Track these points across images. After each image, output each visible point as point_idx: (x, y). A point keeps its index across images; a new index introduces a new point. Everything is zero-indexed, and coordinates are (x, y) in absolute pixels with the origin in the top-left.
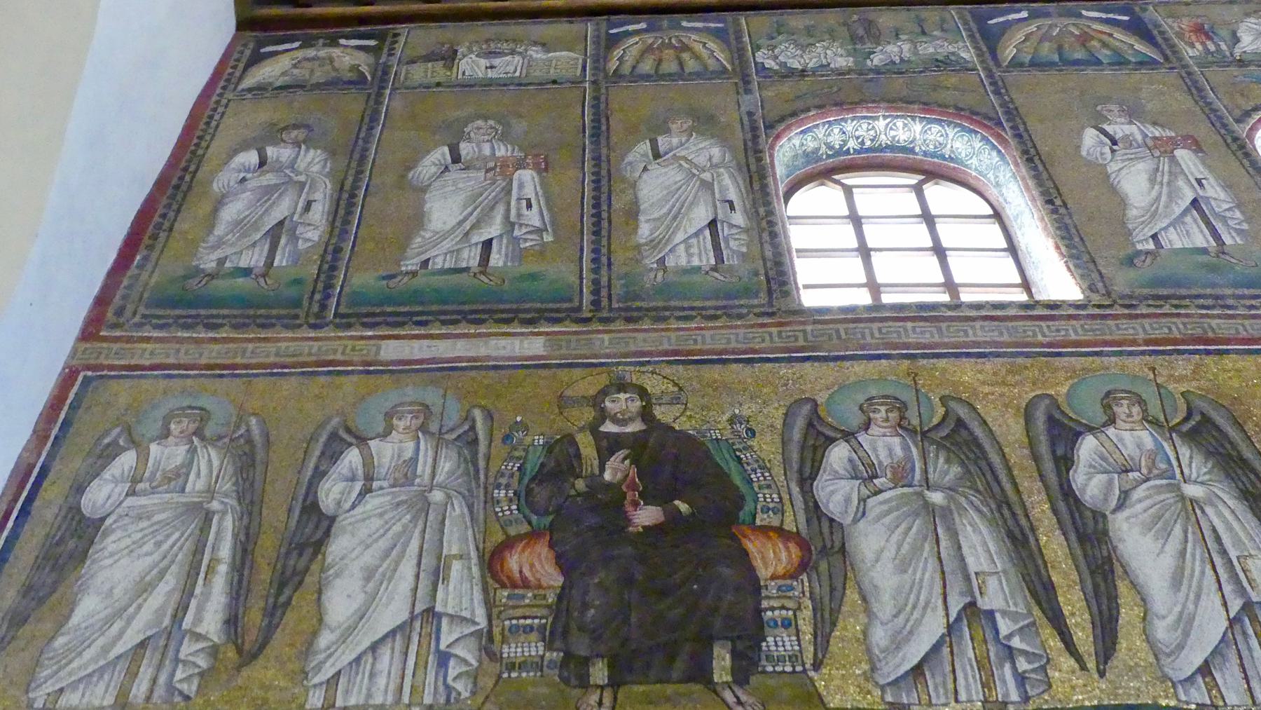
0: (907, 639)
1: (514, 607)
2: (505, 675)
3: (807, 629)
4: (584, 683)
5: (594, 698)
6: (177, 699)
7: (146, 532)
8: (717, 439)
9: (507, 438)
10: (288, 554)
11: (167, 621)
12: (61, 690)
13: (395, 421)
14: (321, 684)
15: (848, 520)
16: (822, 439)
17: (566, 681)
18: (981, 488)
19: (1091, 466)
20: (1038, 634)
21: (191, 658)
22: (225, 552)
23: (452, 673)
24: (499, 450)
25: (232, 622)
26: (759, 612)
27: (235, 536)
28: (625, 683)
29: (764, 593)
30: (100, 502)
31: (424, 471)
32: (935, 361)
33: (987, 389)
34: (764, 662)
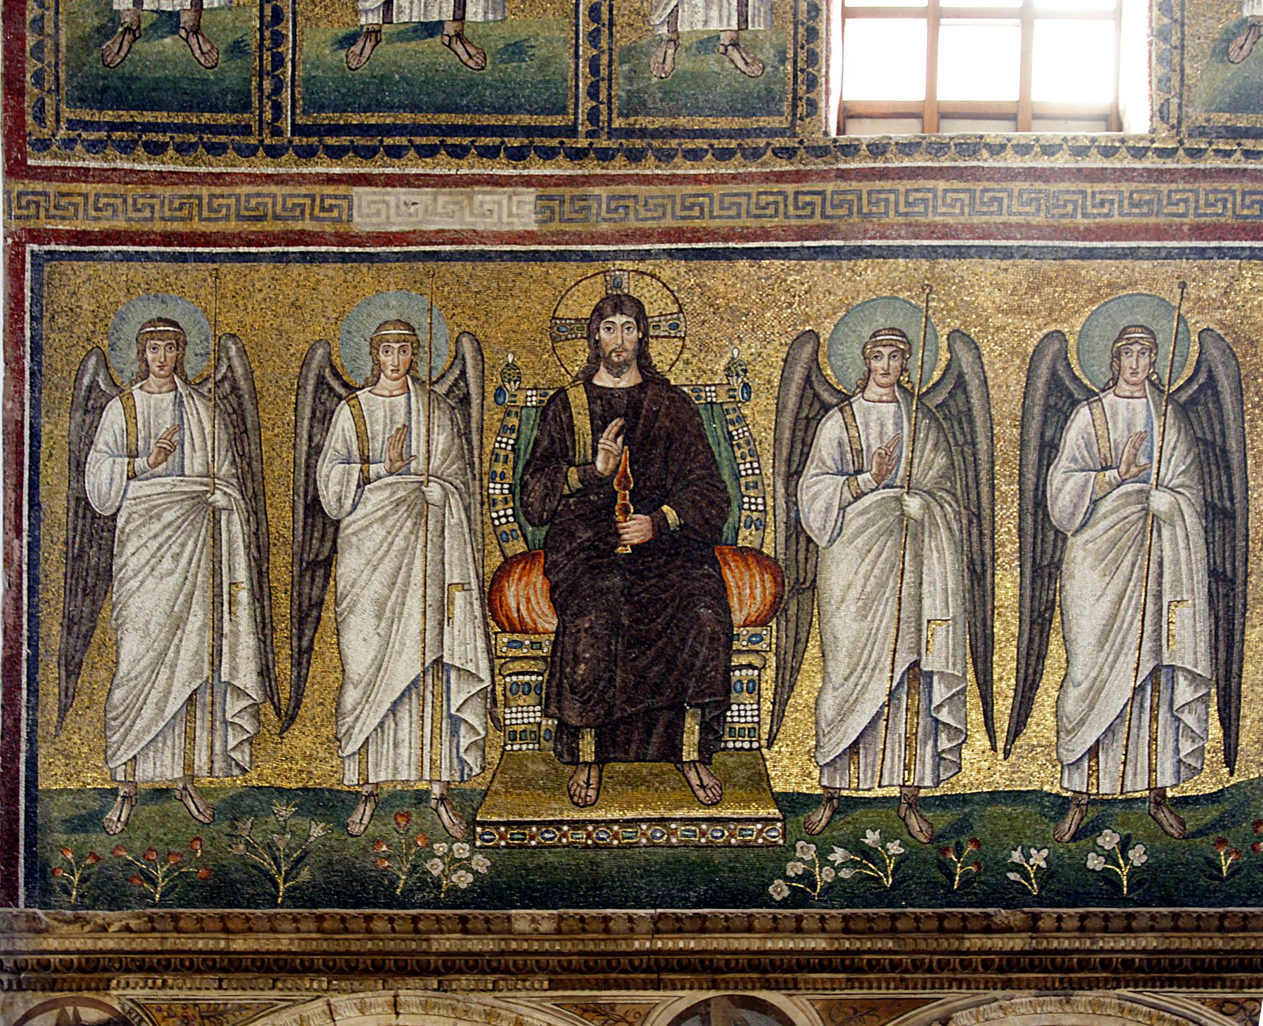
0: (851, 711)
1: (514, 659)
2: (508, 748)
3: (768, 694)
4: (575, 762)
5: (583, 777)
6: (236, 772)
7: (161, 539)
8: (711, 403)
9: (500, 391)
10: (301, 576)
11: (207, 672)
12: (135, 757)
13: (382, 357)
14: (354, 754)
15: (822, 543)
16: (817, 406)
17: (559, 755)
18: (959, 492)
19: (1074, 460)
20: (965, 702)
21: (236, 720)
22: (242, 575)
23: (464, 743)
24: (494, 417)
25: (265, 673)
26: (729, 669)
27: (247, 547)
28: (609, 761)
29: (736, 645)
30: (104, 489)
31: (418, 451)
32: (954, 263)
33: (998, 320)
34: (726, 738)
